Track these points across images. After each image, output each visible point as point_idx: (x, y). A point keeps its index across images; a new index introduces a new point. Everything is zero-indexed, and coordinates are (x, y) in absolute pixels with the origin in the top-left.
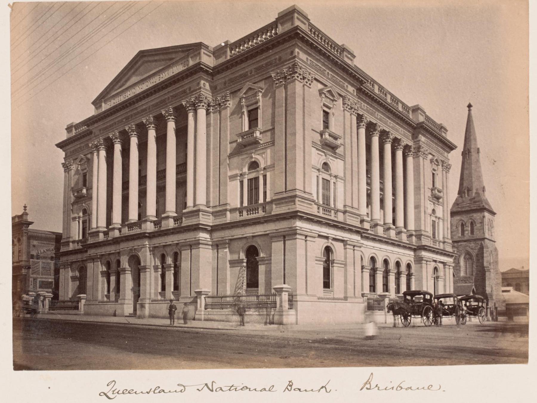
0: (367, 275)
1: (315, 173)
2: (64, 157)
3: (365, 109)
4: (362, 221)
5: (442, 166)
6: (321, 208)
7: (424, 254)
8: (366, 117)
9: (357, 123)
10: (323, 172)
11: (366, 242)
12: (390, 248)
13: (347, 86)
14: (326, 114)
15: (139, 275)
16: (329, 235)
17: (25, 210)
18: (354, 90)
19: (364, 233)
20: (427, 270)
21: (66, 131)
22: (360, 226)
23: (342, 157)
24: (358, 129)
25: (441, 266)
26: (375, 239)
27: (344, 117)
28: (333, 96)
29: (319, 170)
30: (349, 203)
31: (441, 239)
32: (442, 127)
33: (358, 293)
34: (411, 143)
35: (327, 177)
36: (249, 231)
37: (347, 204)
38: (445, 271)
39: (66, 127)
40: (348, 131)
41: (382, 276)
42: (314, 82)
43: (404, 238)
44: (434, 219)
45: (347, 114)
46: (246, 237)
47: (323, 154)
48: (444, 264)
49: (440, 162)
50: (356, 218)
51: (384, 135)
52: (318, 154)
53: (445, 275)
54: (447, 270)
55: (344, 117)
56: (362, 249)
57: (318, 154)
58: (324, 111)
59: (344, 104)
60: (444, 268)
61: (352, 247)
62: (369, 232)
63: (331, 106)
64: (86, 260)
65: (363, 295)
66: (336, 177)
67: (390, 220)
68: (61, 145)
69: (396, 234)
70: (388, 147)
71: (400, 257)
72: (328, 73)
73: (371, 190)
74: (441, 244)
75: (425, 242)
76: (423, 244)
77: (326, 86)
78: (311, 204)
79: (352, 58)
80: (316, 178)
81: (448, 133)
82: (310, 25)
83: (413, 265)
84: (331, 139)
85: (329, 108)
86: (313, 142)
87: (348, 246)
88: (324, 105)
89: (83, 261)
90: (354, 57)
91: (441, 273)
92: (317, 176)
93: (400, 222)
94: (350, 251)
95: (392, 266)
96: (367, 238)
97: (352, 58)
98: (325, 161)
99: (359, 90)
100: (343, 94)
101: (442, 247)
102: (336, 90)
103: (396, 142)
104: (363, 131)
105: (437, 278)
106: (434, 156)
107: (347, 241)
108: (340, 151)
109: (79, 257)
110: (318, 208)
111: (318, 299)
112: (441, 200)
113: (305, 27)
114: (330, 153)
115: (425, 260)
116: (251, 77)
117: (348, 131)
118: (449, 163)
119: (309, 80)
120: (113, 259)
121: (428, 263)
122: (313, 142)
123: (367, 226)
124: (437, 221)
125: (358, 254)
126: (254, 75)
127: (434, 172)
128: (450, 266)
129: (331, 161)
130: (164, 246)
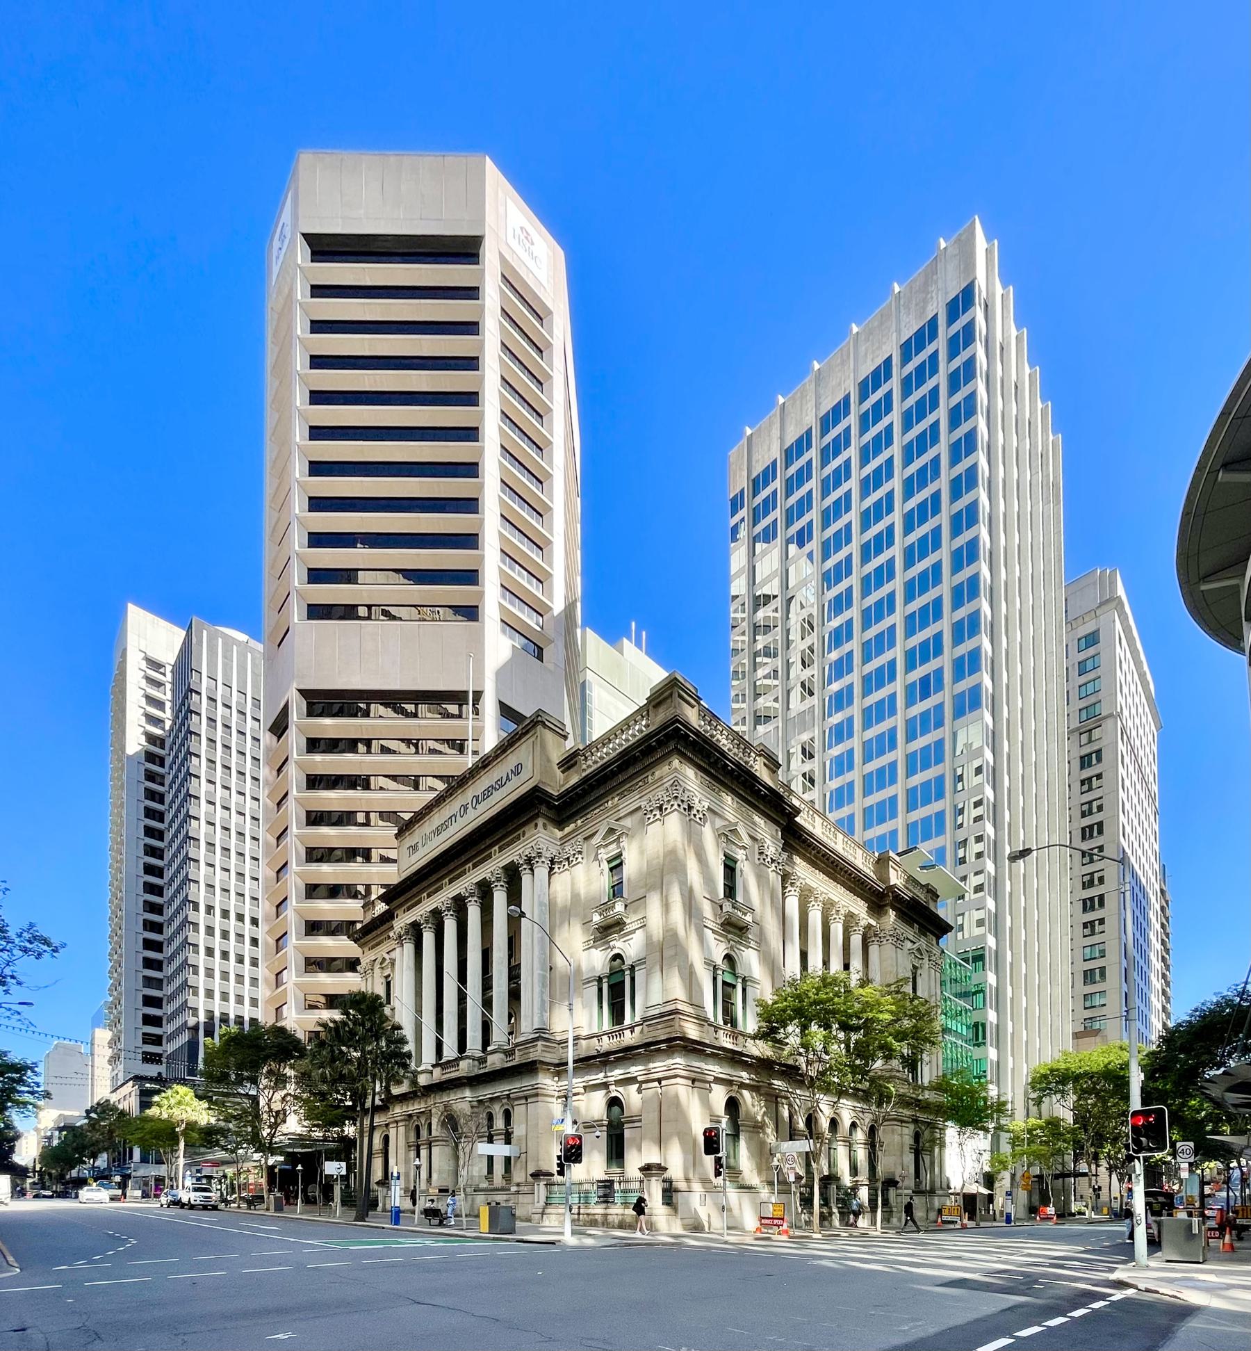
52: (715, 939)
57: (715, 939)
98: (726, 952)
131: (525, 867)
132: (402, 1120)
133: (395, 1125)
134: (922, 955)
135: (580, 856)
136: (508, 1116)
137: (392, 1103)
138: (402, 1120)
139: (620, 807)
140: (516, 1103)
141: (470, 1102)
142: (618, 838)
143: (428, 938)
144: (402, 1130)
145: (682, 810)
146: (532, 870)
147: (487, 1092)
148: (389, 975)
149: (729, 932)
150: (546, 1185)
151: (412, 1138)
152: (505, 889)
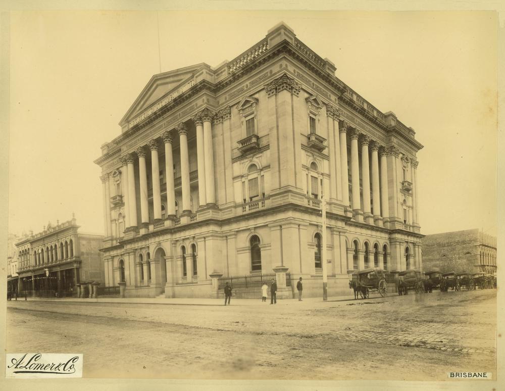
0: (351, 256)
1: (305, 172)
2: (101, 171)
3: (346, 115)
4: (346, 211)
5: (411, 163)
6: (311, 202)
7: (398, 236)
8: (346, 123)
9: (339, 128)
10: (311, 171)
11: (347, 228)
12: (369, 232)
13: (330, 95)
14: (312, 120)
15: (165, 263)
16: (318, 224)
17: (74, 216)
18: (336, 99)
19: (347, 221)
20: (400, 250)
21: (101, 150)
22: (344, 215)
23: (327, 157)
24: (340, 133)
25: (411, 246)
26: (357, 225)
27: (328, 122)
28: (318, 104)
29: (308, 169)
30: (334, 196)
31: (411, 224)
32: (410, 131)
33: (345, 270)
34: (383, 145)
35: (315, 175)
36: (252, 223)
37: (332, 197)
38: (414, 251)
39: (101, 146)
40: (331, 134)
41: (363, 256)
42: (301, 91)
43: (381, 224)
44: (405, 208)
45: (331, 120)
46: (249, 229)
47: (311, 155)
48: (414, 244)
49: (410, 161)
50: (340, 209)
51: (362, 138)
53: (415, 253)
54: (417, 249)
55: (328, 122)
56: (346, 234)
57: (307, 155)
58: (310, 117)
59: (327, 111)
60: (414, 247)
61: (338, 233)
62: (352, 220)
63: (317, 113)
64: (124, 254)
65: (348, 272)
66: (322, 174)
67: (368, 209)
68: (99, 162)
69: (374, 222)
70: (366, 149)
71: (378, 240)
72: (313, 83)
73: (351, 186)
74: (411, 228)
75: (398, 227)
76: (397, 229)
77: (311, 95)
78: (303, 198)
79: (333, 71)
80: (306, 176)
81: (415, 135)
82: (296, 40)
83: (388, 247)
84: (317, 142)
85: (315, 115)
86: (302, 144)
87: (335, 233)
88: (311, 112)
89: (121, 255)
90: (335, 69)
91: (412, 252)
92: (307, 174)
93: (377, 212)
94: (336, 237)
95: (371, 248)
96: (350, 225)
97: (333, 71)
98: (312, 161)
99: (340, 98)
100: (327, 102)
101: (411, 231)
102: (321, 98)
103: (372, 144)
104: (344, 135)
105: (407, 257)
106: (404, 155)
107: (334, 227)
108: (325, 152)
109: (119, 252)
110: (309, 202)
111: (312, 277)
112: (410, 192)
113: (292, 42)
114: (318, 154)
115: (398, 242)
116: (246, 90)
117: (331, 134)
118: (417, 160)
119: (297, 90)
120: (144, 252)
121: (401, 244)
122: (302, 144)
123: (350, 215)
124: (407, 210)
125: (343, 239)
126: (250, 88)
127: (404, 168)
128: (419, 246)
129: (318, 161)
130: (184, 240)
131: (198, 122)
132: (132, 252)
133: (128, 254)
134: (408, 160)
135: (229, 115)
136: (194, 247)
137: (125, 244)
138: (132, 252)
139: (252, 89)
140: (199, 240)
141: (171, 241)
142: (252, 105)
143: (142, 161)
144: (132, 257)
145: (288, 89)
146: (202, 123)
147: (179, 236)
148: (119, 180)
149: (314, 151)
150: (218, 280)
151: (138, 260)
152: (210, 121)
